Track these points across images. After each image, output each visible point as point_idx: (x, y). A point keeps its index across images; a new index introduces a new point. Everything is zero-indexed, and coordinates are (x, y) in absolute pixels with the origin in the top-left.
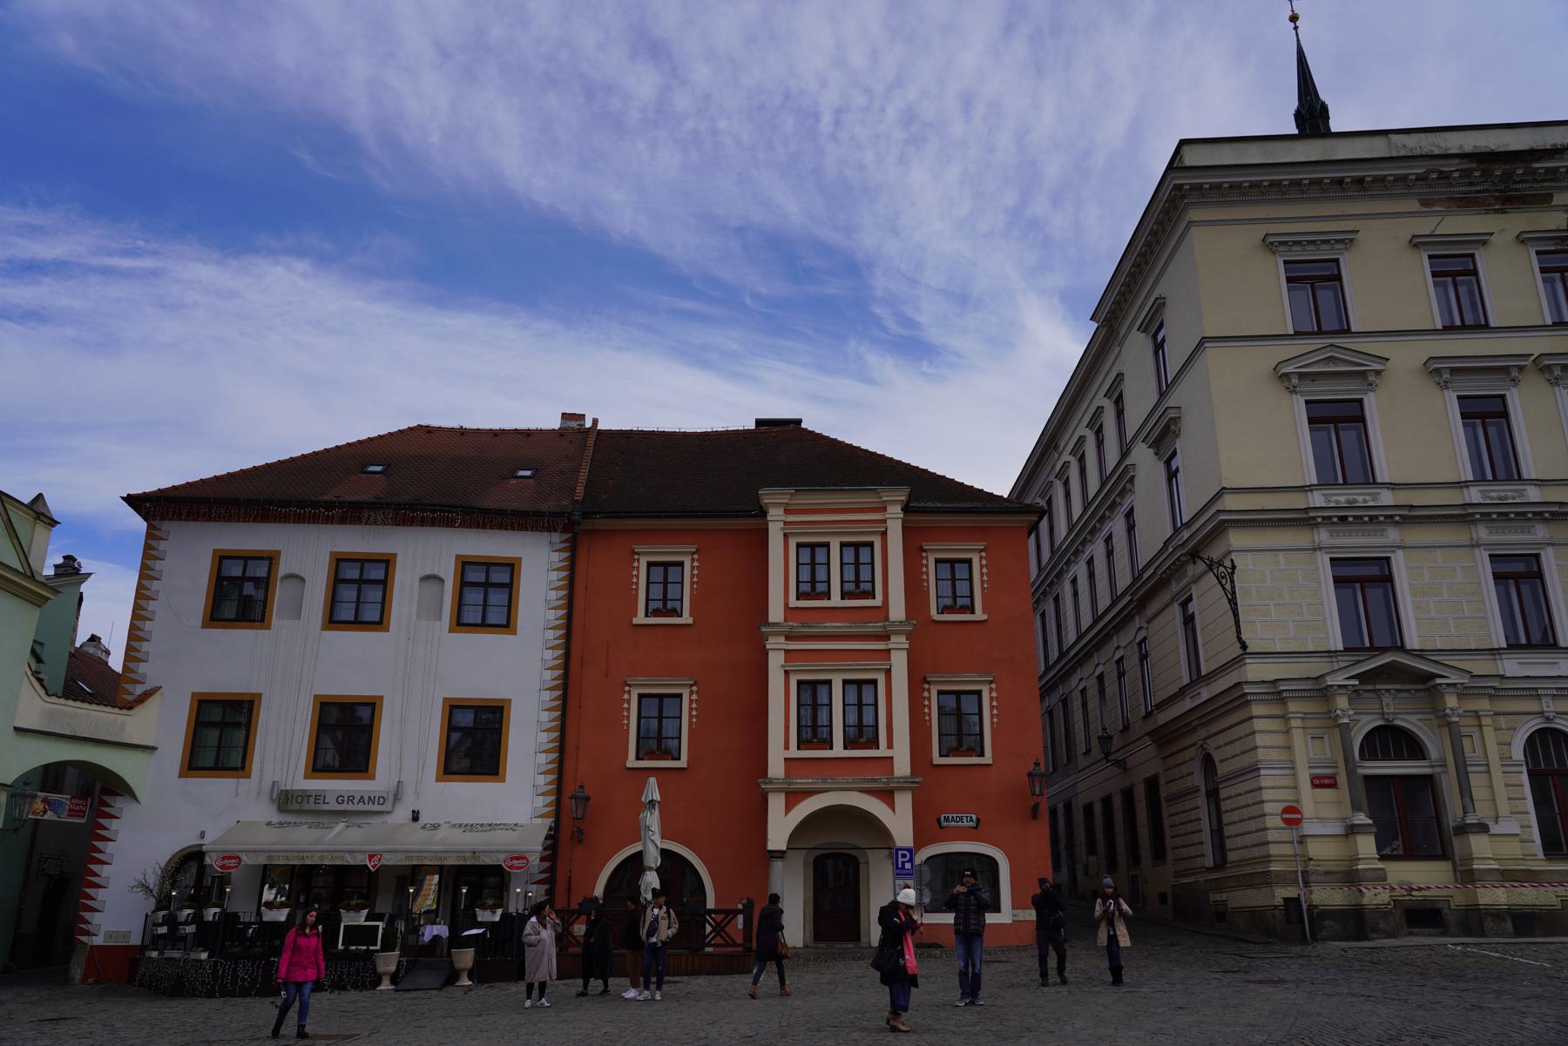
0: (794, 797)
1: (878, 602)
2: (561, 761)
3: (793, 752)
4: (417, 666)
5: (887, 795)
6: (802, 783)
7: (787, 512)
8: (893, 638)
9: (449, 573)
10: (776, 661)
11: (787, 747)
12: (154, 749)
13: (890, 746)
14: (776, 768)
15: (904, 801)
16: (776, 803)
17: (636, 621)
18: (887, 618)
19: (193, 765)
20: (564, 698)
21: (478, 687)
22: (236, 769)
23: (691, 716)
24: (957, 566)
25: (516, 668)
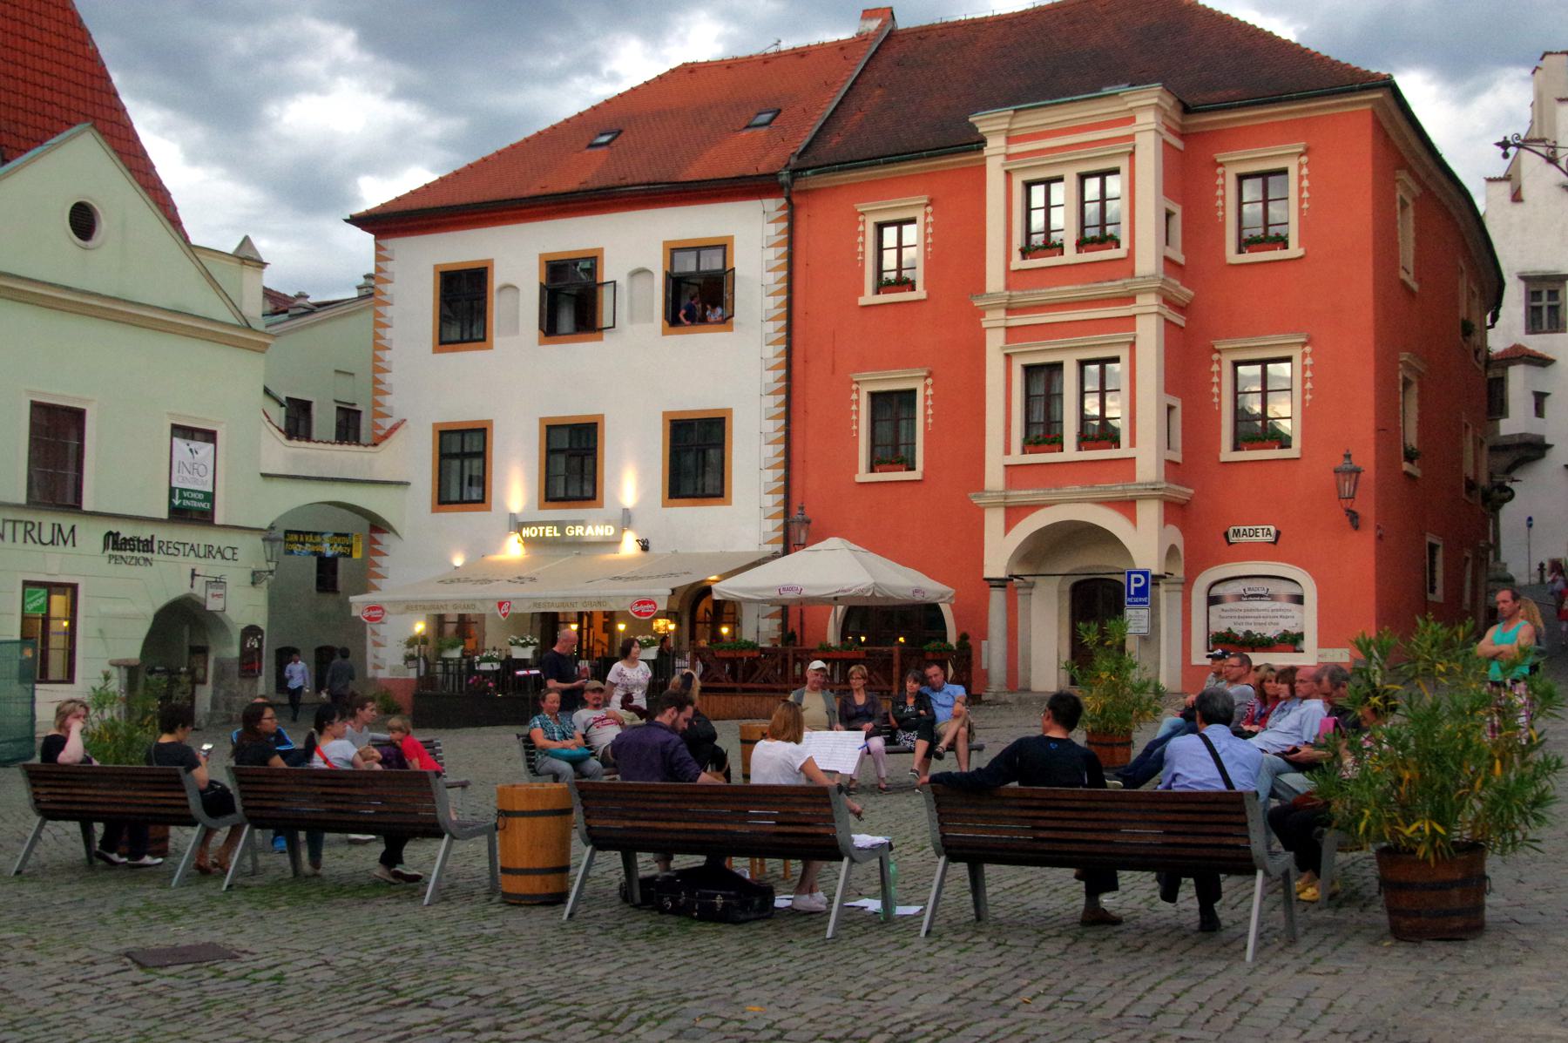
0: (1014, 514)
1: (1120, 253)
2: (788, 479)
3: (1017, 457)
4: (637, 376)
5: (1126, 506)
6: (1021, 495)
7: (1010, 140)
8: (1140, 300)
9: (657, 265)
10: (995, 344)
11: (1008, 451)
12: (407, 484)
13: (1133, 444)
14: (994, 477)
15: (1150, 513)
16: (994, 521)
17: (862, 301)
18: (1132, 274)
19: (443, 500)
20: (788, 403)
21: (696, 400)
22: (589, 499)
23: (926, 417)
24: (1271, 179)
25: (730, 375)
